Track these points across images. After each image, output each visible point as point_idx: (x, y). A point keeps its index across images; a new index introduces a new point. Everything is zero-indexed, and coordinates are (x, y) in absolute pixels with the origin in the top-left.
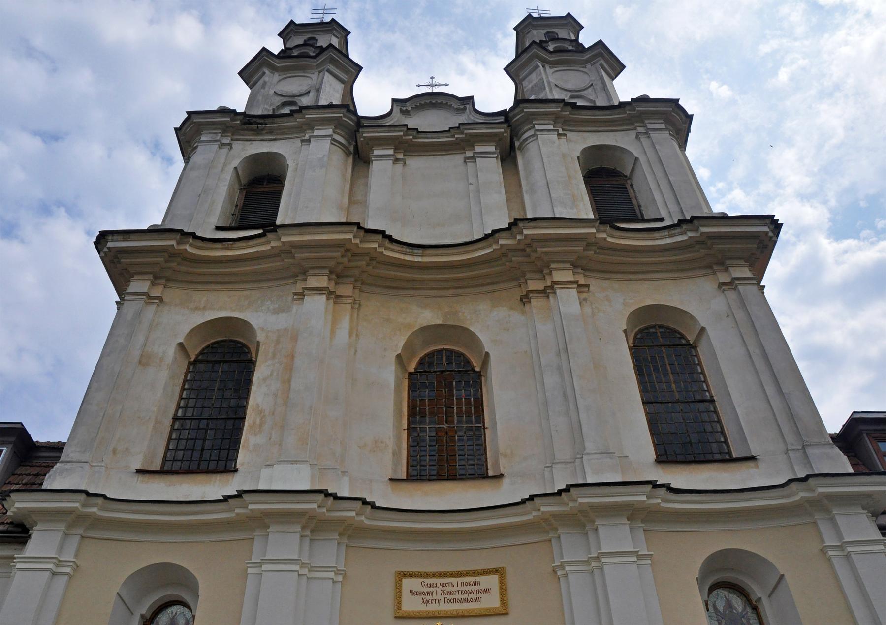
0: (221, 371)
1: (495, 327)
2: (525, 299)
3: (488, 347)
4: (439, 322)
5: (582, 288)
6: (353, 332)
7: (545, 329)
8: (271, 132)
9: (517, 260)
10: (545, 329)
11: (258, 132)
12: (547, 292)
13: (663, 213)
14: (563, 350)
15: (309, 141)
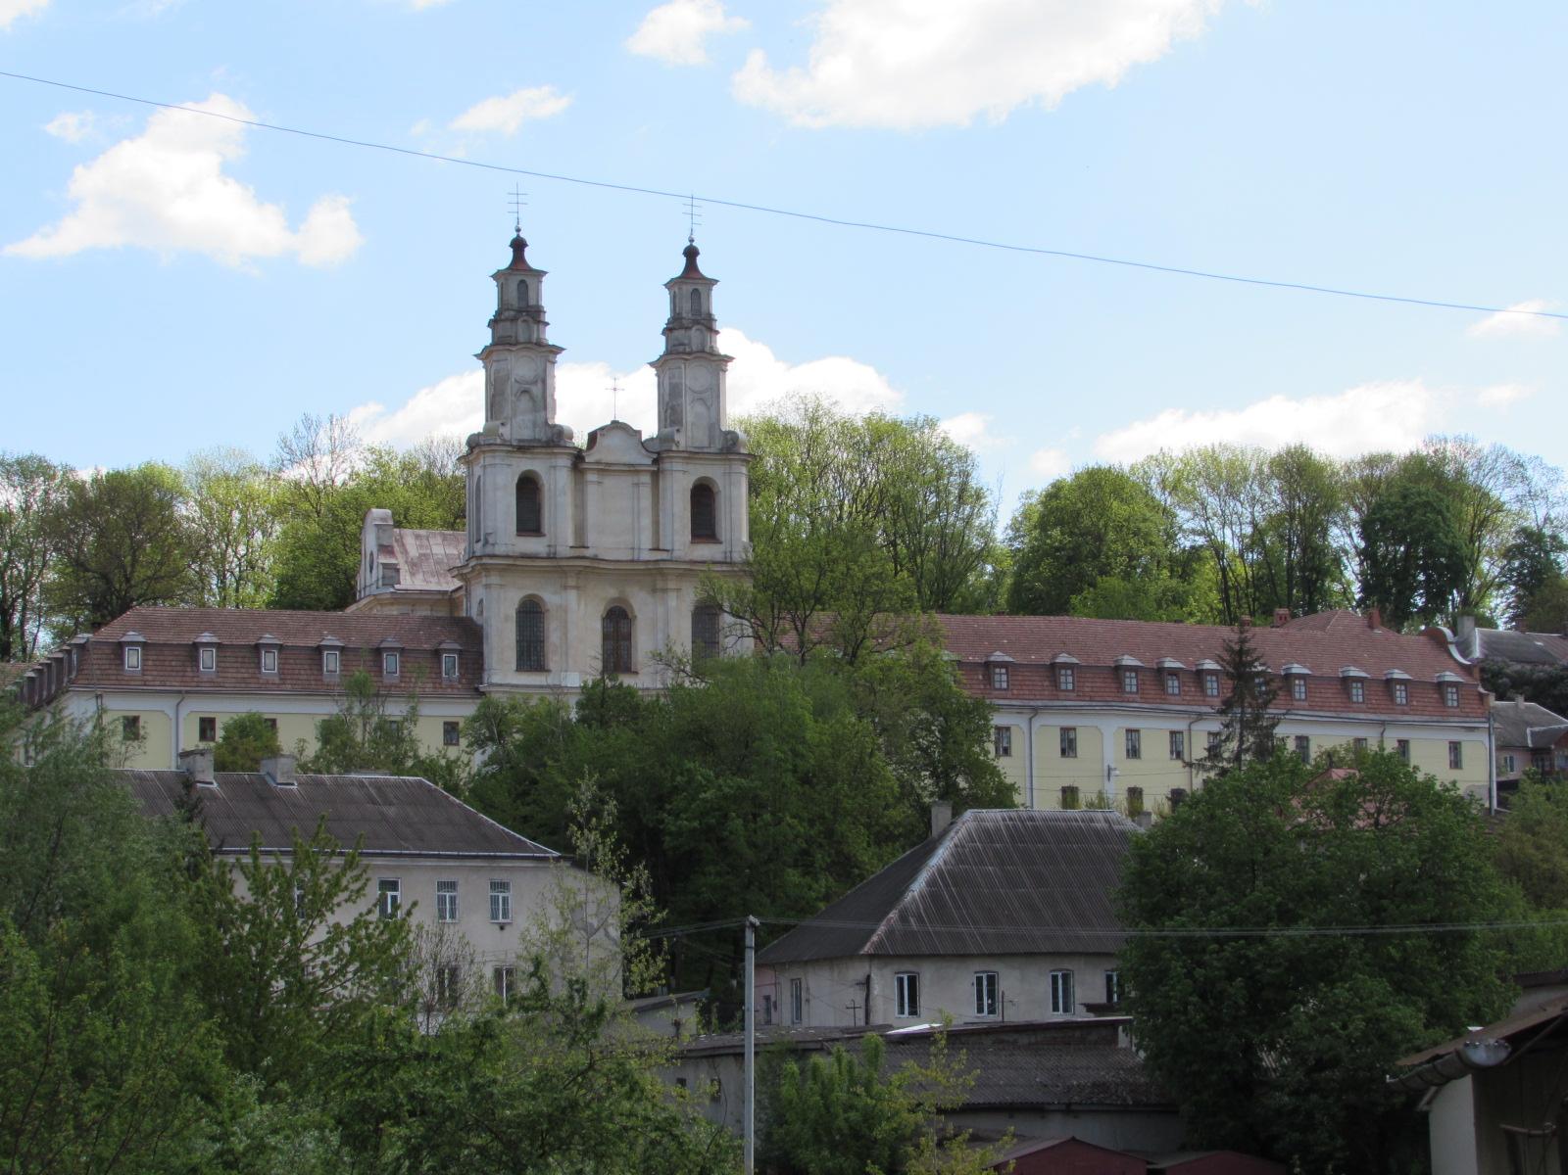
0: (531, 615)
1: (641, 604)
2: (654, 591)
3: (637, 613)
4: (617, 595)
5: (678, 590)
6: (586, 605)
7: (660, 610)
8: (532, 453)
9: (655, 574)
10: (660, 610)
11: (524, 453)
12: (665, 590)
13: (723, 539)
14: (667, 623)
15: (555, 467)
